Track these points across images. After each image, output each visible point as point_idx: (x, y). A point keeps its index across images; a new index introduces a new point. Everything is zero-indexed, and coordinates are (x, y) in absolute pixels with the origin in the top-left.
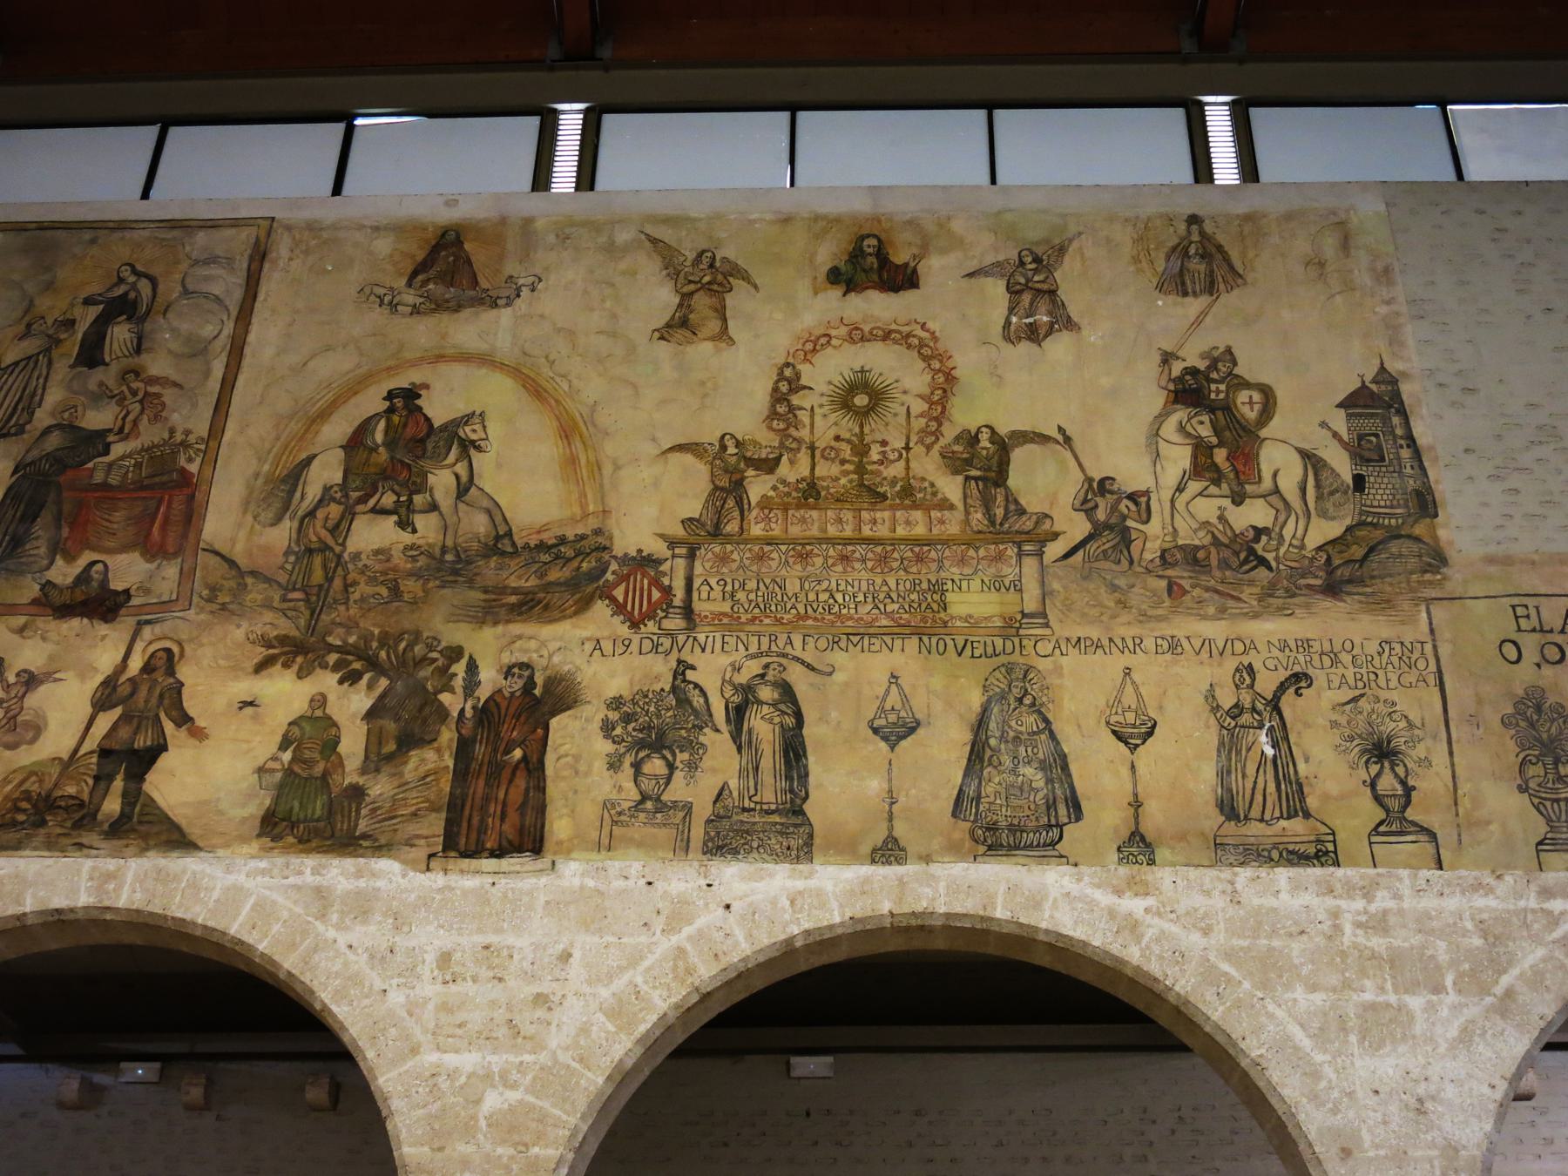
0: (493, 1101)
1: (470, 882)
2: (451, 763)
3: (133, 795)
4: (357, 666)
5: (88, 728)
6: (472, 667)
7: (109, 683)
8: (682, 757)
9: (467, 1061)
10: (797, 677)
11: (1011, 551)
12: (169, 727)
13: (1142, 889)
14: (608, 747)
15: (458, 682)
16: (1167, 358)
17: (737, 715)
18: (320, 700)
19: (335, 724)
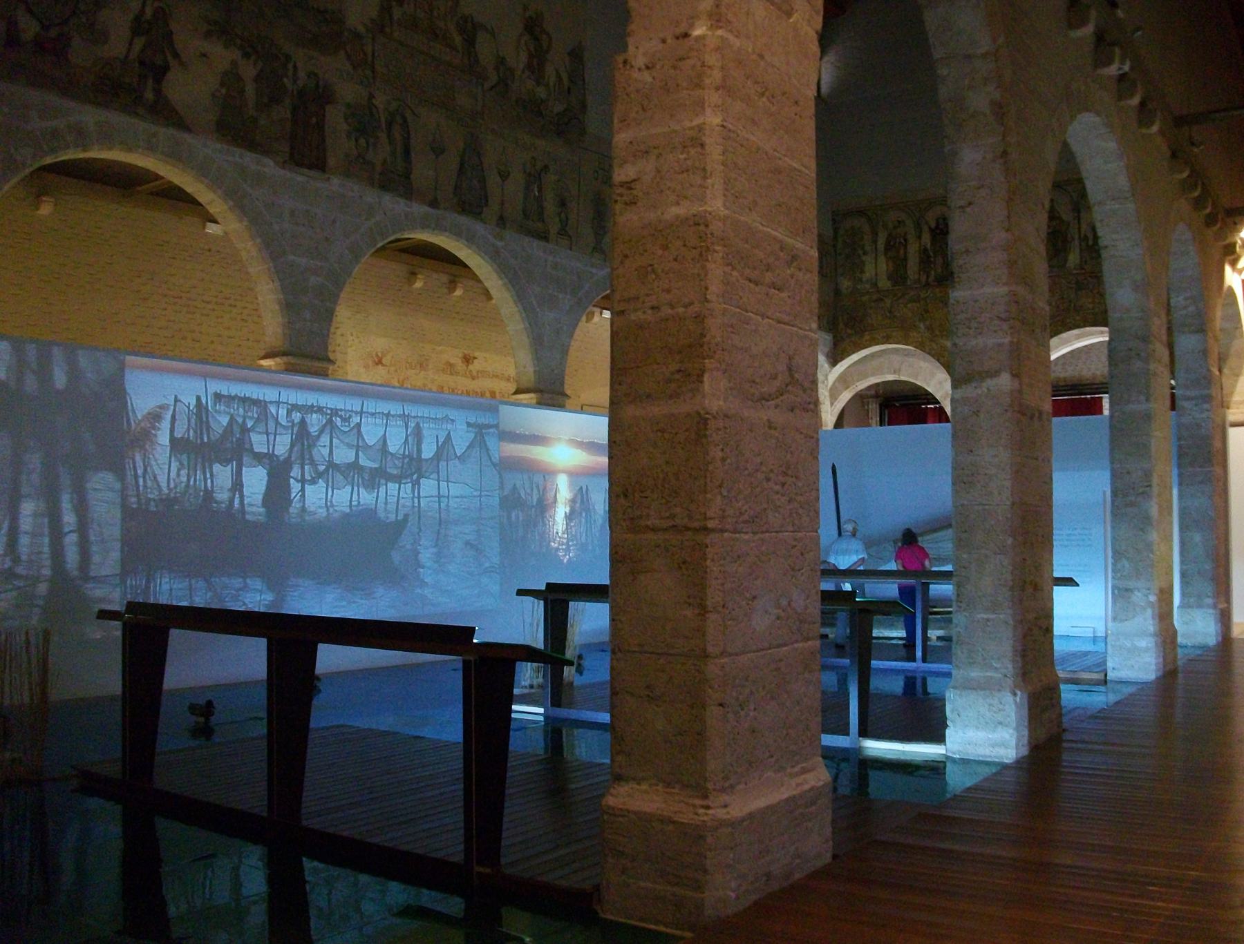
0: (314, 280)
1: (300, 179)
2: (289, 116)
3: (158, 92)
4: (249, 50)
5: (131, 44)
6: (295, 67)
7: (137, 19)
8: (372, 140)
9: (303, 261)
10: (408, 114)
11: (475, 80)
12: (169, 58)
13: (501, 239)
14: (345, 127)
15: (290, 73)
16: (525, 8)
17: (390, 125)
18: (234, 63)
19: (242, 80)
